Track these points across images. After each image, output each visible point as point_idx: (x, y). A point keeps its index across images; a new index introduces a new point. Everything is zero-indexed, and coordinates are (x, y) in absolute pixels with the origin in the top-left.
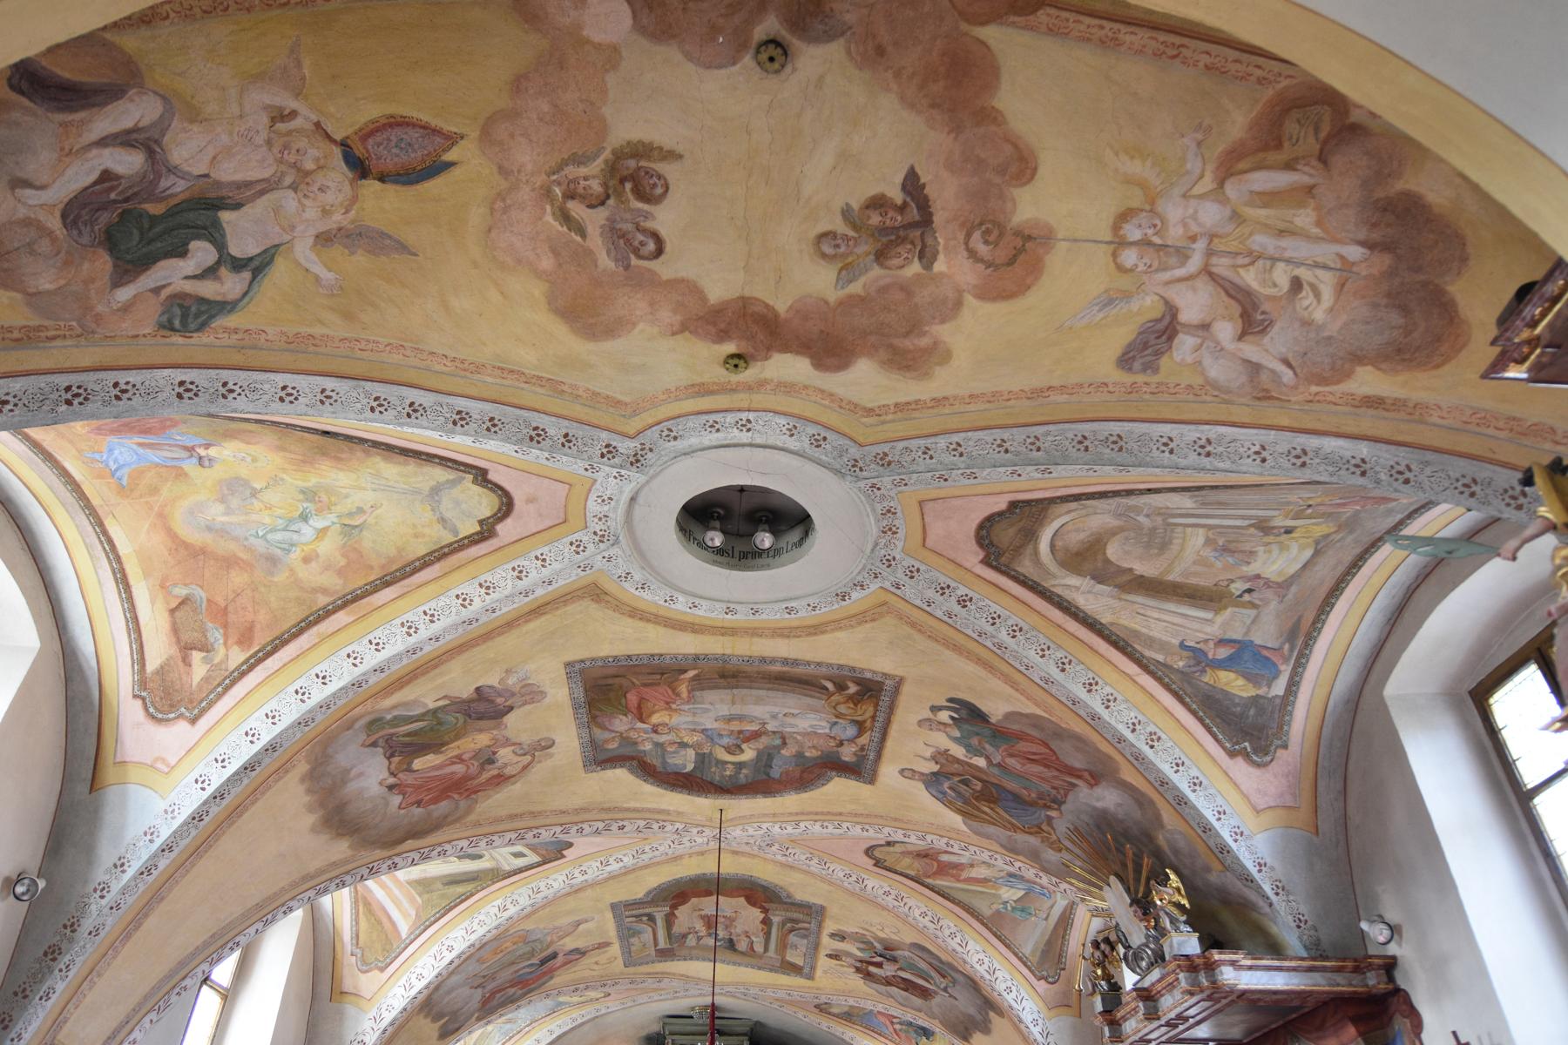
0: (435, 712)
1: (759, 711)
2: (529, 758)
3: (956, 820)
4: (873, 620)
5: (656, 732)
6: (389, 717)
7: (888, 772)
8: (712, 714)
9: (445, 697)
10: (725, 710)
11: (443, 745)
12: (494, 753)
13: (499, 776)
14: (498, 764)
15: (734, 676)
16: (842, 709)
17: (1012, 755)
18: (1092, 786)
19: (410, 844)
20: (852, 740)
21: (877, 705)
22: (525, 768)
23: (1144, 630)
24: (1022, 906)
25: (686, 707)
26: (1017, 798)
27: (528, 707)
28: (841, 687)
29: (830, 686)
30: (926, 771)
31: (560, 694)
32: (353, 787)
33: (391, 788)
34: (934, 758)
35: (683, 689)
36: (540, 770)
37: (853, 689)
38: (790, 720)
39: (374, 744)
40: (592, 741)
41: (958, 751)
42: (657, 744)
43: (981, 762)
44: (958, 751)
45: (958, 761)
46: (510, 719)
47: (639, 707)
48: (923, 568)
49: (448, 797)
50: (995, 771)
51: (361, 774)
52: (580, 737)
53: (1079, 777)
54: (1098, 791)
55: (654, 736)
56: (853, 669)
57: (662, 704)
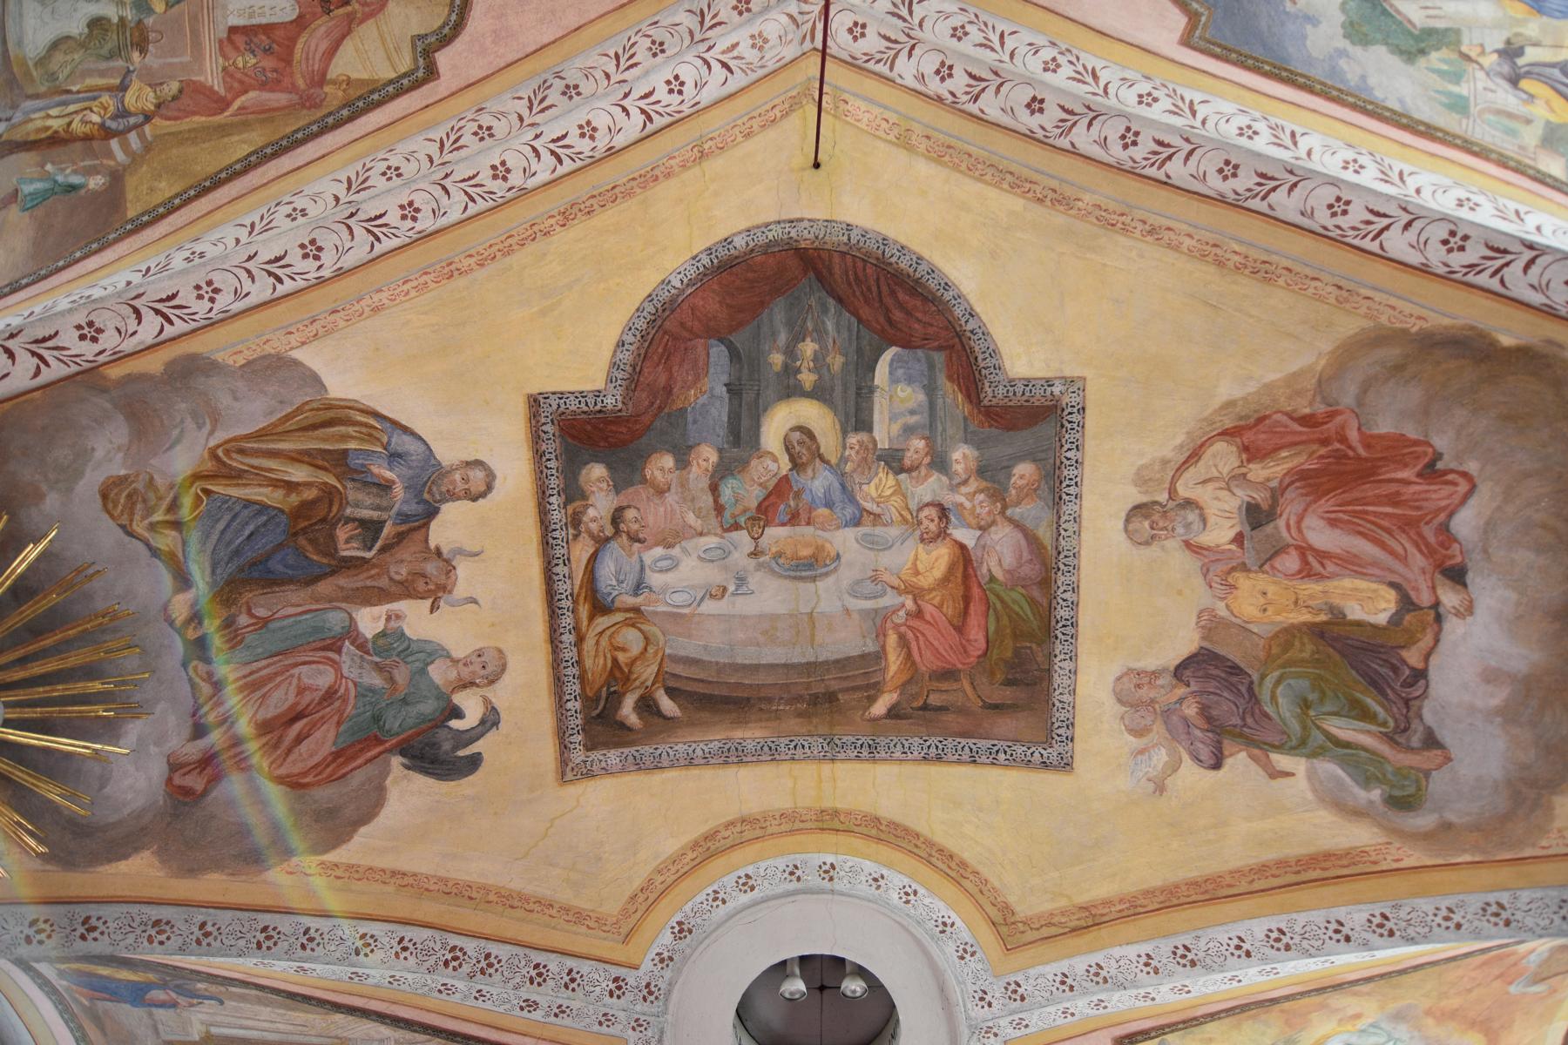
0: (1300, 747)
1: (770, 596)
2: (1183, 491)
3: (344, 375)
4: (634, 897)
5: (943, 512)
6: (1376, 794)
8: (846, 575)
9: (1276, 774)
10: (827, 595)
11: (1318, 632)
12: (1239, 539)
13: (1252, 453)
14: (1243, 495)
15: (815, 700)
16: (631, 639)
17: (330, 695)
18: (175, 766)
19: (1510, 332)
20: (601, 542)
21: (582, 678)
22: (1194, 456)
25: (890, 600)
27: (1150, 663)
28: (646, 705)
29: (667, 705)
30: (451, 513)
31: (1092, 681)
32: (1521, 656)
33: (1457, 576)
35: (894, 661)
36: (1167, 443)
37: (628, 711)
38: (712, 575)
39: (1431, 741)
40: (1057, 501)
41: (417, 620)
42: (940, 463)
43: (369, 621)
44: (417, 620)
45: (407, 590)
46: (1184, 642)
47: (967, 599)
48: (596, 1028)
49: (1368, 441)
50: (335, 620)
51: (1491, 676)
52: (1077, 520)
54: (157, 769)
55: (949, 499)
56: (639, 766)
57: (929, 609)
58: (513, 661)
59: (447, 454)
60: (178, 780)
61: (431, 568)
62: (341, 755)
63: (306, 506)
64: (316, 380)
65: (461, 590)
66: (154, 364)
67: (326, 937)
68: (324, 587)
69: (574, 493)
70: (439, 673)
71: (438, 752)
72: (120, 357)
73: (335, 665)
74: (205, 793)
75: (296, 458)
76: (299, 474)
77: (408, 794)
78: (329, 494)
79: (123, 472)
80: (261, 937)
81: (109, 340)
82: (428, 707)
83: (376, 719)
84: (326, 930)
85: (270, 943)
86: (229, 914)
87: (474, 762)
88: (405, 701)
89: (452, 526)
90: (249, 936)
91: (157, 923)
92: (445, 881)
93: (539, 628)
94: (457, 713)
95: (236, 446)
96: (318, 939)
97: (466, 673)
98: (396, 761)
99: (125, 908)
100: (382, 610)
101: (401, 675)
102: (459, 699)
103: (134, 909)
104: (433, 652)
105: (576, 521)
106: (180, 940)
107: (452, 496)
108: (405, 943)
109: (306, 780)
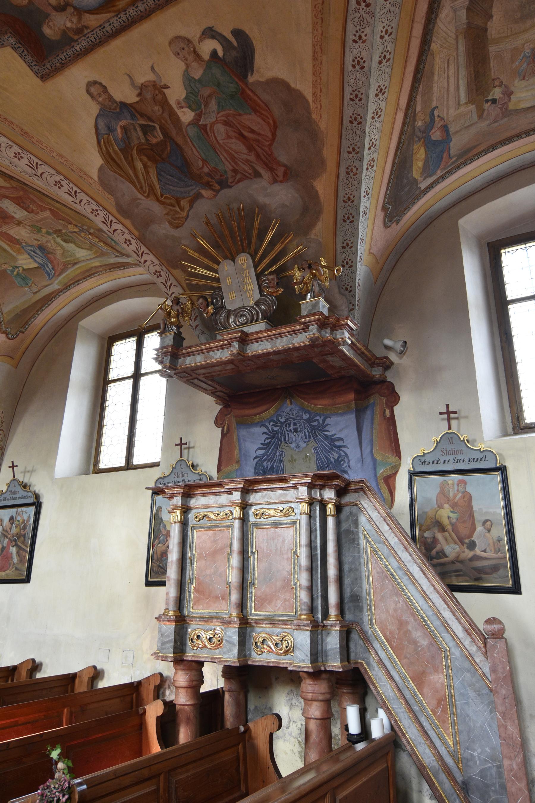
3: (93, 161)
7: (77, 77)
17: (227, 123)
18: (275, 181)
20: (80, 11)
23: (436, 78)
24: (26, 276)
26: (185, 169)
30: (118, 96)
34: (142, 89)
41: (176, 93)
43: (186, 116)
44: (176, 93)
45: (164, 103)
50: (192, 132)
53: (271, 170)
54: (277, 187)
58: (172, 33)
59: (95, 109)
60: (281, 178)
61: (148, 96)
62: (255, 109)
63: (149, 158)
64: (101, 169)
65: (151, 77)
66: (127, 222)
67: (355, 88)
68: (180, 140)
69: (67, 39)
70: (197, 73)
71: (239, 55)
72: (131, 232)
73: (212, 125)
74: (285, 166)
75: (134, 169)
76: (139, 165)
77: (268, 66)
78: (140, 151)
79: (167, 224)
80: (355, 123)
81: (127, 236)
82: (217, 71)
83: (232, 97)
84: (351, 89)
85: (358, 118)
86: (343, 141)
87: (238, 33)
88: (218, 85)
89: (124, 94)
90: (354, 129)
91: (347, 173)
92: (314, 24)
93: (145, 27)
94: (214, 53)
95: (141, 189)
96: (356, 92)
97: (191, 58)
98: (251, 79)
99: (340, 187)
100: (179, 112)
101: (206, 92)
102: (206, 56)
103: (341, 183)
104: (188, 80)
105: (79, 31)
106: (357, 161)
107: (111, 98)
108: (357, 38)
109: (271, 122)
